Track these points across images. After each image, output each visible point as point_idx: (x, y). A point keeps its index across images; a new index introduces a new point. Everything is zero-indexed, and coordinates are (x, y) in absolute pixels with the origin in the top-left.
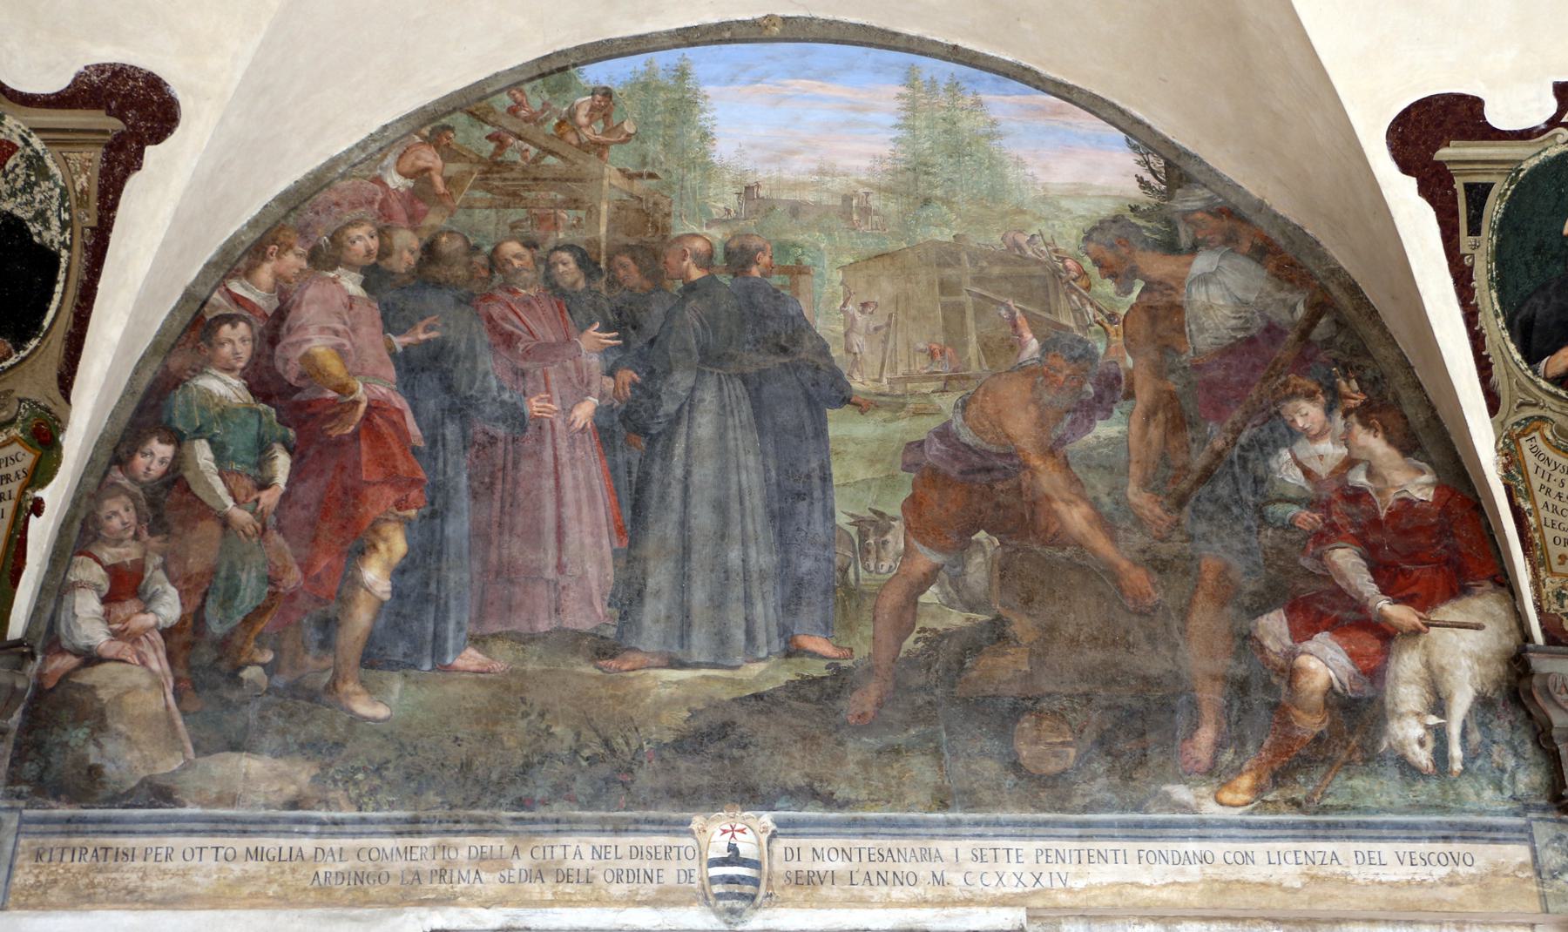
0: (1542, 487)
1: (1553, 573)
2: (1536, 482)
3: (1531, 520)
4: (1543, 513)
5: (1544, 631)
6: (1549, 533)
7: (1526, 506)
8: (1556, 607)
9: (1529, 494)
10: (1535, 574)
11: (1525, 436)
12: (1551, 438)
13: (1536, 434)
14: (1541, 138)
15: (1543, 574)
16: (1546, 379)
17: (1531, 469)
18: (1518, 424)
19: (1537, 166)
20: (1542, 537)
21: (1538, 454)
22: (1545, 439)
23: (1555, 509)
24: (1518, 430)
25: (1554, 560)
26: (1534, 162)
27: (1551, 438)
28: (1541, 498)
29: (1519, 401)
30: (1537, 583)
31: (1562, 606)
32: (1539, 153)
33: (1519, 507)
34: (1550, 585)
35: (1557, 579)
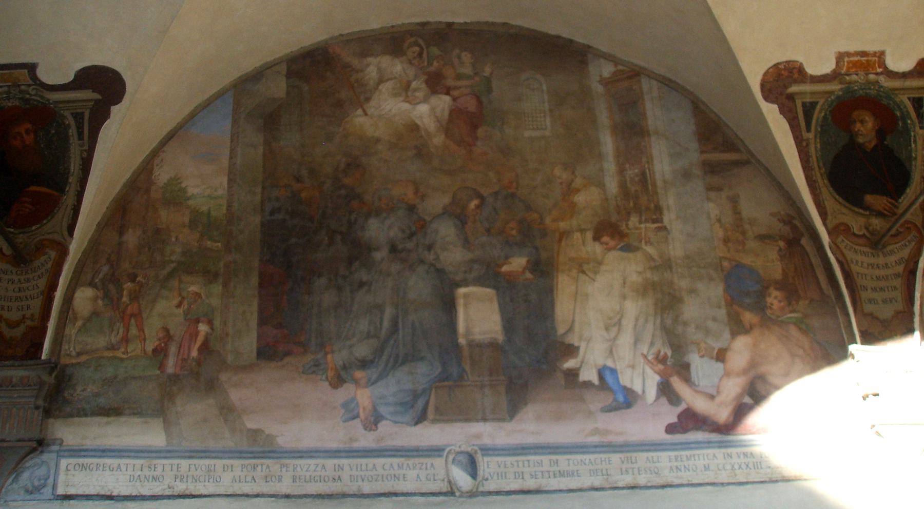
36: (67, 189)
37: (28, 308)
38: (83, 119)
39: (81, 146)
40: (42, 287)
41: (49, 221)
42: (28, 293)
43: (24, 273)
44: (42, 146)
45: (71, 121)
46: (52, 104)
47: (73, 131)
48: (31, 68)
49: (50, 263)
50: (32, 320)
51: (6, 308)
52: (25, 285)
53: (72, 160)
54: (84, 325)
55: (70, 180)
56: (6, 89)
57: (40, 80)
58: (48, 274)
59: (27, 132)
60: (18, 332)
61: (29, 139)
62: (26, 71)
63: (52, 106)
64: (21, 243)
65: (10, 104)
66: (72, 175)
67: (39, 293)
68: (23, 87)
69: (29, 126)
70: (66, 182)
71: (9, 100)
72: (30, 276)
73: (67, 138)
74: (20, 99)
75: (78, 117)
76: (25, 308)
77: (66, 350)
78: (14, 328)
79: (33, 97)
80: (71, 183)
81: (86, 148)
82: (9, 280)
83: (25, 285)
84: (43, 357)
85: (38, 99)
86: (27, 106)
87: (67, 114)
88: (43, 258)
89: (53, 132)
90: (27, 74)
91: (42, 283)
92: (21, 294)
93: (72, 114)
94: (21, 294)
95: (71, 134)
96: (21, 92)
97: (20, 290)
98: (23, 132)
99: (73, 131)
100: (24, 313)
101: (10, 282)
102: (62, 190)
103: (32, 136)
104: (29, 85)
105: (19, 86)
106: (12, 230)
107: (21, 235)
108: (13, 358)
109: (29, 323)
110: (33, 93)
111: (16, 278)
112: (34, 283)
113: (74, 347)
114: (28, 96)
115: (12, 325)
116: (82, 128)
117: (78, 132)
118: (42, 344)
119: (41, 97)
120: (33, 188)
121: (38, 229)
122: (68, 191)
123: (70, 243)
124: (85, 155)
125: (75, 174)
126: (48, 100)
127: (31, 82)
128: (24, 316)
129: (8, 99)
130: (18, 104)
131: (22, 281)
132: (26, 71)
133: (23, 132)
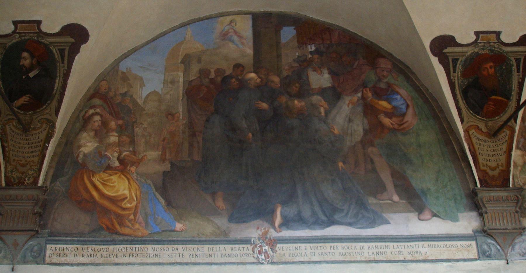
0: (11, 139)
1: (10, 164)
2: (10, 137)
3: (7, 149)
4: (11, 147)
5: (5, 182)
6: (11, 152)
7: (6, 145)
8: (10, 175)
9: (7, 141)
10: (6, 165)
11: (8, 124)
12: (15, 125)
13: (11, 124)
14: (11, 37)
15: (8, 165)
16: (15, 107)
17: (8, 134)
18: (6, 120)
19: (11, 45)
20: (9, 154)
21: (11, 130)
22: (13, 125)
23: (14, 146)
24: (6, 122)
25: (12, 161)
26: (10, 44)
27: (15, 125)
28: (10, 142)
29: (7, 114)
30: (6, 168)
31: (12, 174)
32: (11, 41)
33: (4, 145)
34: (10, 168)
35: (12, 166)
36: (511, 98)
37: (499, 160)
38: (520, 61)
39: (518, 75)
40: (505, 150)
41: (504, 114)
42: (499, 152)
43: (495, 142)
44: (498, 75)
45: (514, 62)
46: (505, 53)
47: (514, 68)
48: (498, 34)
49: (507, 137)
50: (502, 167)
51: (488, 160)
52: (496, 148)
53: (513, 83)
54: (522, 169)
55: (513, 94)
56: (483, 44)
57: (501, 40)
58: (507, 143)
59: (491, 67)
60: (496, 173)
61: (491, 71)
62: (495, 35)
63: (505, 54)
64: (491, 126)
65: (483, 52)
66: (514, 91)
67: (504, 153)
68: (492, 44)
69: (492, 64)
70: (510, 94)
71: (483, 50)
72: (498, 143)
73: (511, 71)
74: (489, 50)
75: (518, 60)
76: (498, 160)
77: (517, 182)
78: (493, 170)
79: (496, 49)
80: (513, 95)
81: (521, 76)
82: (488, 145)
83: (496, 148)
84: (511, 186)
85: (499, 50)
86: (492, 54)
87: (513, 59)
88: (503, 134)
89: (504, 68)
90: (495, 37)
91: (505, 147)
92: (495, 153)
93: (515, 59)
94: (495, 153)
95: (513, 69)
96: (490, 46)
97: (494, 151)
98: (488, 67)
99: (514, 68)
100: (497, 163)
101: (488, 147)
102: (509, 99)
103: (493, 70)
104: (495, 43)
105: (490, 43)
106: (485, 119)
107: (490, 122)
108: (496, 186)
109: (501, 168)
110: (497, 46)
111: (491, 144)
112: (501, 147)
113: (521, 181)
114: (493, 48)
115: (493, 169)
116: (519, 66)
117: (517, 68)
118: (509, 179)
119: (500, 49)
120: (493, 97)
121: (499, 118)
122: (512, 99)
123: (516, 126)
124: (520, 80)
125: (515, 90)
126: (504, 51)
127: (496, 41)
128: (498, 164)
129: (483, 49)
130: (488, 52)
131: (494, 146)
132: (495, 35)
133: (488, 67)
